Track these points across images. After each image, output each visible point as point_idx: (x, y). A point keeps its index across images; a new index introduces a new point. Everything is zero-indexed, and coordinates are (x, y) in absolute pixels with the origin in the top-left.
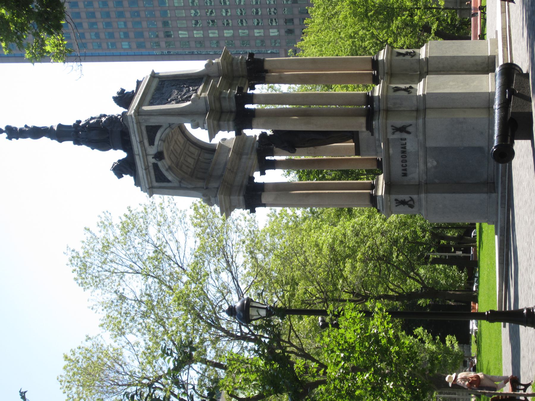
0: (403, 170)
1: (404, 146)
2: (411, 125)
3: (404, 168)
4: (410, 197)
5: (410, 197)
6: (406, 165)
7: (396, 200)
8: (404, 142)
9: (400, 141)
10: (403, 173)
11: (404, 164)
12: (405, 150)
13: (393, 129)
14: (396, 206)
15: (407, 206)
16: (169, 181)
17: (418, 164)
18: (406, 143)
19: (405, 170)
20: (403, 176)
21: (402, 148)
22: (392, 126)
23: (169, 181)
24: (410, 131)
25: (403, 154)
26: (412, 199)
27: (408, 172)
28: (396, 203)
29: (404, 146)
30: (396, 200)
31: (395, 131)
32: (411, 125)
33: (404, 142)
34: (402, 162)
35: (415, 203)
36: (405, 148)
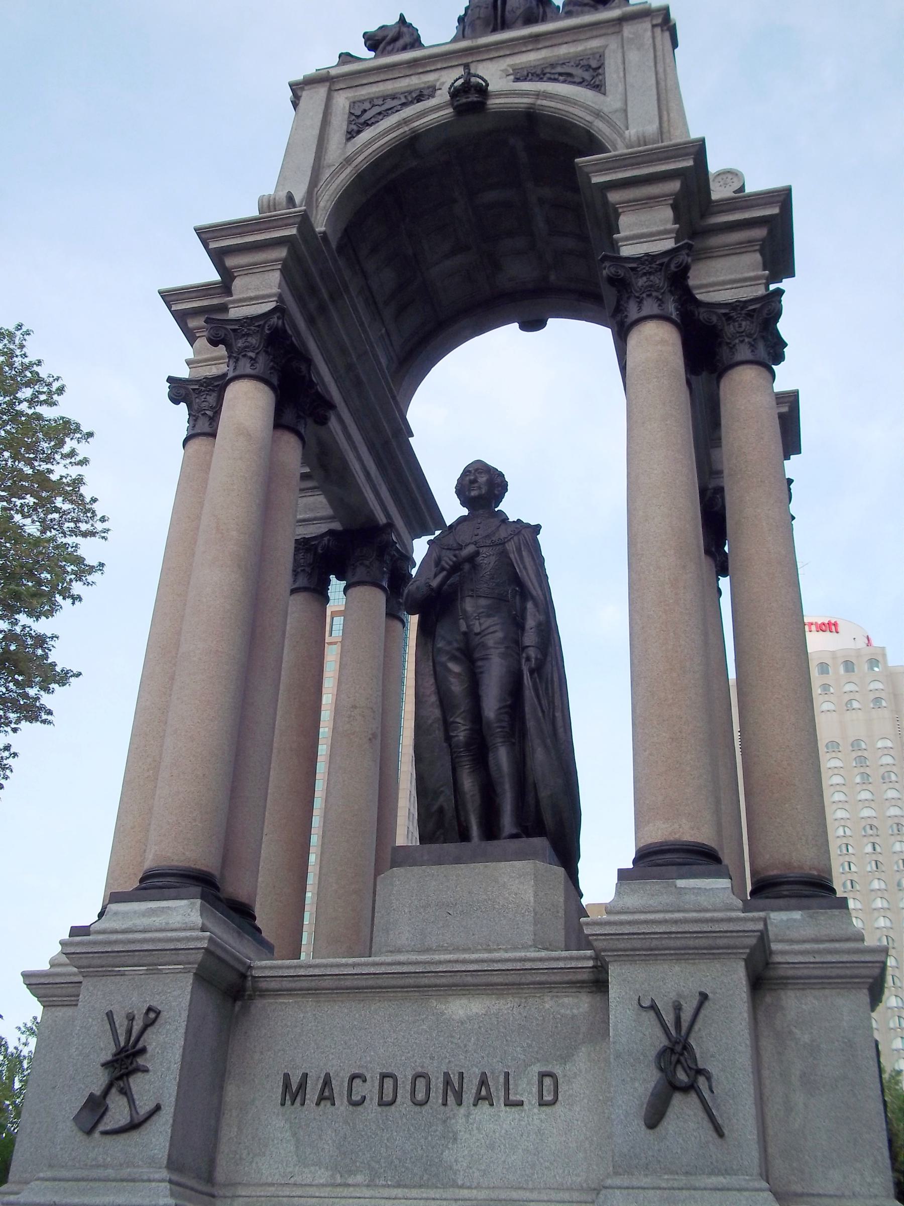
0: (327, 1082)
1: (499, 1095)
2: (719, 1131)
3: (339, 1087)
4: (158, 1108)
5: (158, 1108)
6: (364, 1098)
7: (152, 1016)
8: (525, 1089)
9: (536, 1069)
10: (305, 1076)
11: (368, 1089)
12: (469, 1096)
13: (678, 1008)
14: (110, 1015)
15: (97, 1081)
16: (351, 135)
17: (359, 1178)
18: (520, 1104)
19: (326, 1096)
20: (287, 1077)
21: (483, 1082)
22: (704, 997)
23: (351, 135)
24: (670, 1124)
25: (438, 1084)
26: (133, 1126)
27: (310, 1109)
28: (131, 1018)
29: (499, 1095)
30: (152, 1016)
31: (669, 1019)
32: (719, 1131)
33: (525, 1089)
34: (383, 1076)
35: (108, 1140)
36: (483, 1097)
